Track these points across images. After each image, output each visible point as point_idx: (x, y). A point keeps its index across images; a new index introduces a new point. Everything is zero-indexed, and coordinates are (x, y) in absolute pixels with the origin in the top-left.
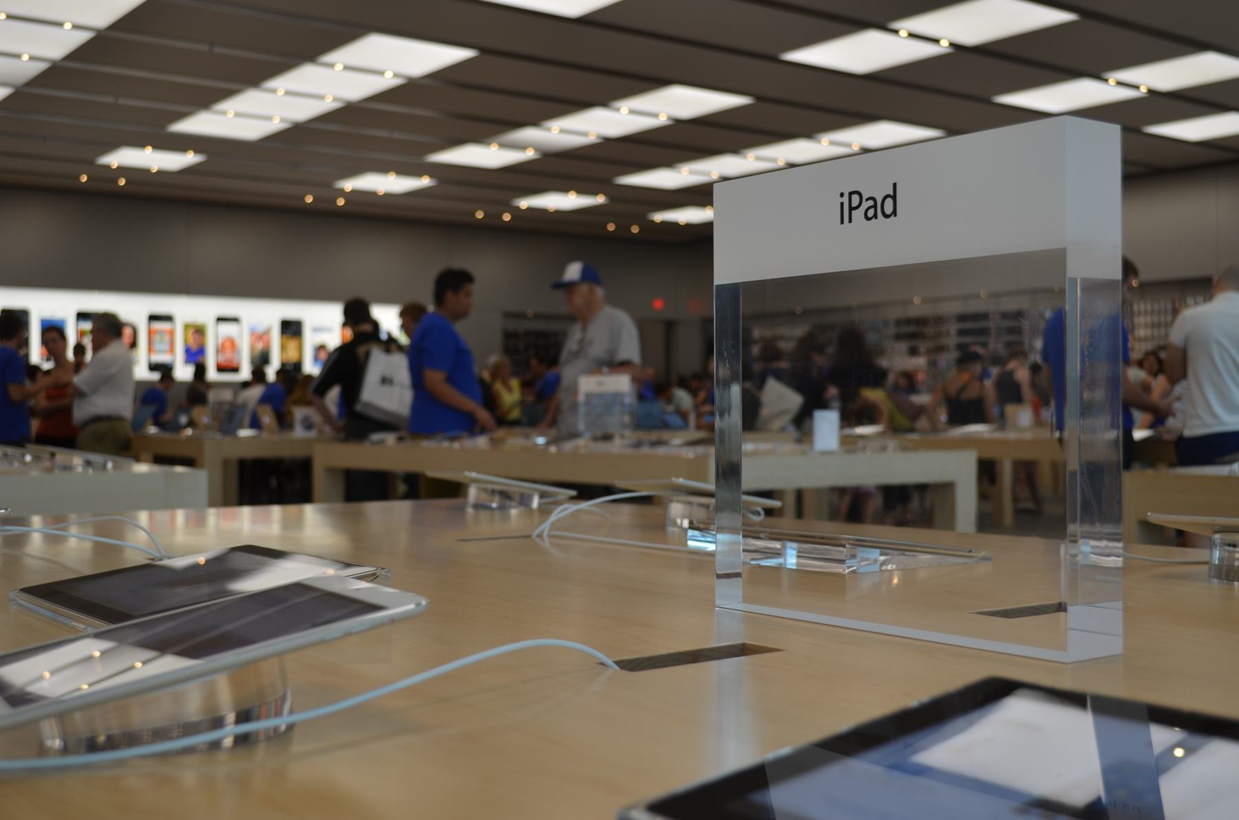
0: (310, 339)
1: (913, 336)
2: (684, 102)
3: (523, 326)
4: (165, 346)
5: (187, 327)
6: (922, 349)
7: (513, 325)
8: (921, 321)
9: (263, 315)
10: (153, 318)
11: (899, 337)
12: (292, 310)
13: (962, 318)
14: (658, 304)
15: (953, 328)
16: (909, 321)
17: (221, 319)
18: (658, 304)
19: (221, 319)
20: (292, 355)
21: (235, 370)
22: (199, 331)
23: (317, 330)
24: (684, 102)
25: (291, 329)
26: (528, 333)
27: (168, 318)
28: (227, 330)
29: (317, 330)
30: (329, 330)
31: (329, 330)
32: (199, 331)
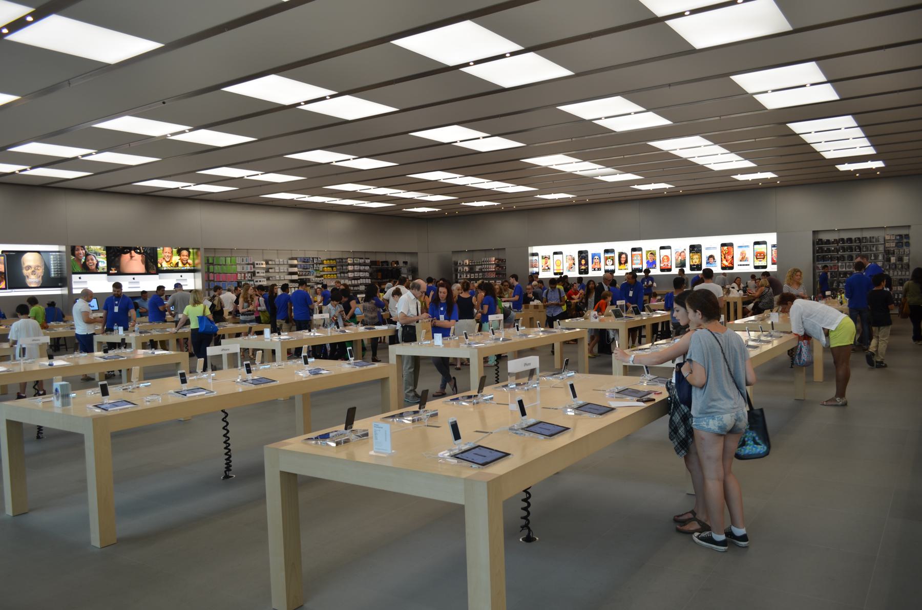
0: (705, 254)
2: (740, 177)
4: (639, 262)
5: (648, 252)
9: (681, 245)
10: (634, 250)
12: (695, 241)
17: (662, 248)
19: (662, 248)
20: (696, 261)
21: (670, 270)
22: (653, 254)
23: (707, 249)
24: (740, 177)
25: (695, 249)
26: (836, 241)
27: (640, 249)
28: (664, 252)
29: (707, 249)
30: (715, 248)
31: (715, 248)
32: (653, 254)
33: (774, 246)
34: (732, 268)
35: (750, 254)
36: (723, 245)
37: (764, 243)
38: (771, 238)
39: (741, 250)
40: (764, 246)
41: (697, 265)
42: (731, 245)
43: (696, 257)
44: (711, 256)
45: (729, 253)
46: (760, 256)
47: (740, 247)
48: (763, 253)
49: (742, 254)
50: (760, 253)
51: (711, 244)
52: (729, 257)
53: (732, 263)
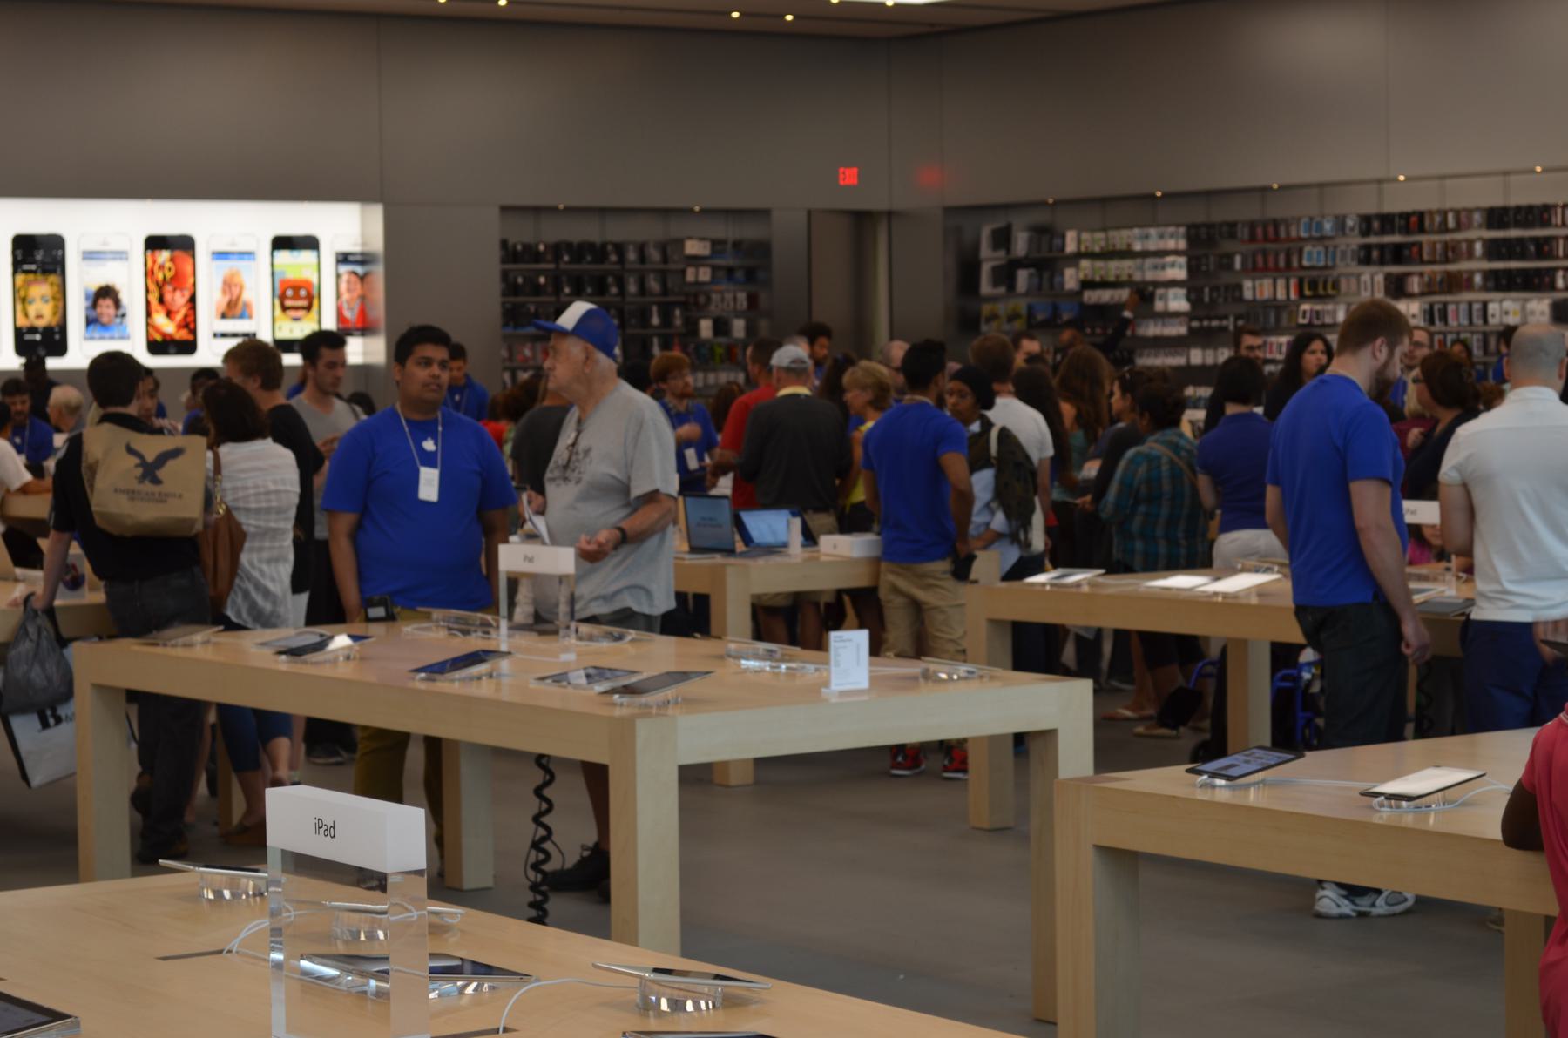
0: (80, 279)
1: (1397, 254)
3: (550, 233)
6: (1415, 285)
7: (522, 233)
8: (1414, 221)
13: (1496, 217)
14: (849, 176)
15: (1479, 234)
16: (1387, 222)
18: (849, 176)
20: (41, 313)
23: (89, 256)
26: (556, 249)
30: (121, 255)
31: (121, 255)
33: (343, 258)
34: (189, 347)
35: (259, 293)
36: (155, 243)
37: (310, 243)
38: (346, 226)
39: (226, 266)
40: (306, 256)
41: (48, 332)
42: (184, 245)
43: (41, 290)
44: (106, 293)
45: (177, 280)
46: (296, 297)
47: (220, 255)
48: (307, 285)
49: (229, 285)
50: (296, 287)
51: (105, 237)
52: (179, 300)
53: (190, 324)
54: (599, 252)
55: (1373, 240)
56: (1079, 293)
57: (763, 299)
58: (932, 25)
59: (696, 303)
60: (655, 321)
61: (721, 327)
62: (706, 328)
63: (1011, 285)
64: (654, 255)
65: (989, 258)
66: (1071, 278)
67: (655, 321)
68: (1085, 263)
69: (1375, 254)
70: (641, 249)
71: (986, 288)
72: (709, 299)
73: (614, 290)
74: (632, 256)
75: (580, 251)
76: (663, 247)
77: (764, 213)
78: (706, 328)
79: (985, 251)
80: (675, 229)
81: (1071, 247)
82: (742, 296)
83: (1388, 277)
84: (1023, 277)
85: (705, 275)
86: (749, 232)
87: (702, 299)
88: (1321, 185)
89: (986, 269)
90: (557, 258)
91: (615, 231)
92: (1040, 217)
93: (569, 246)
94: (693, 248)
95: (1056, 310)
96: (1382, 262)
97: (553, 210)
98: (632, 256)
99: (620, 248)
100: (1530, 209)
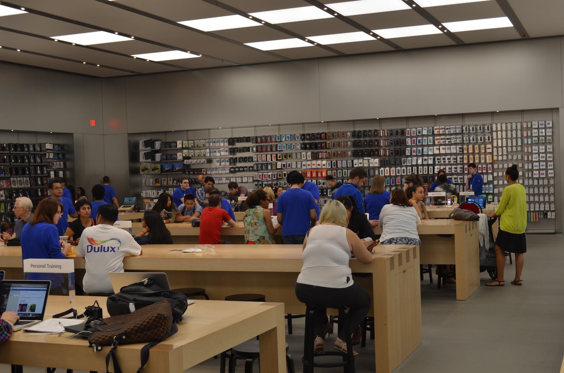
1: (316, 146)
3: (14, 140)
11: (304, 147)
54: (22, 146)
55: (306, 142)
56: (183, 161)
57: (68, 165)
58: (133, 72)
59: (49, 166)
60: (39, 172)
61: (56, 174)
62: (52, 173)
63: (153, 159)
64: (38, 148)
65: (143, 150)
66: (180, 156)
67: (39, 172)
68: (185, 151)
69: (308, 146)
70: (34, 146)
71: (142, 159)
72: (53, 164)
73: (27, 161)
74: (31, 149)
75: (16, 146)
76: (40, 145)
77: (71, 135)
78: (52, 173)
79: (141, 147)
80: (41, 140)
81: (179, 146)
82: (62, 163)
83: (312, 153)
84: (158, 157)
85: (51, 156)
86: (61, 141)
87: (51, 164)
88: (187, 131)
89: (142, 154)
90: (10, 149)
91: (23, 140)
92: (148, 138)
93: (13, 144)
94: (49, 146)
95: (173, 167)
96: (310, 148)
97: (9, 131)
98: (31, 149)
99: (28, 146)
100: (240, 138)
